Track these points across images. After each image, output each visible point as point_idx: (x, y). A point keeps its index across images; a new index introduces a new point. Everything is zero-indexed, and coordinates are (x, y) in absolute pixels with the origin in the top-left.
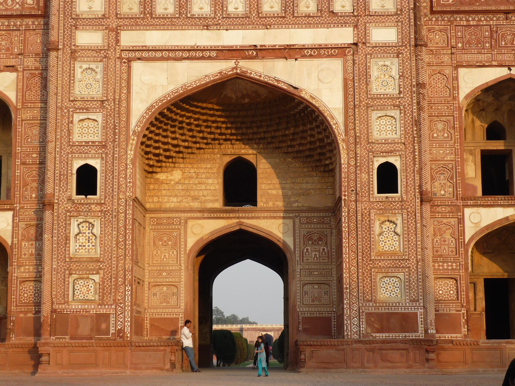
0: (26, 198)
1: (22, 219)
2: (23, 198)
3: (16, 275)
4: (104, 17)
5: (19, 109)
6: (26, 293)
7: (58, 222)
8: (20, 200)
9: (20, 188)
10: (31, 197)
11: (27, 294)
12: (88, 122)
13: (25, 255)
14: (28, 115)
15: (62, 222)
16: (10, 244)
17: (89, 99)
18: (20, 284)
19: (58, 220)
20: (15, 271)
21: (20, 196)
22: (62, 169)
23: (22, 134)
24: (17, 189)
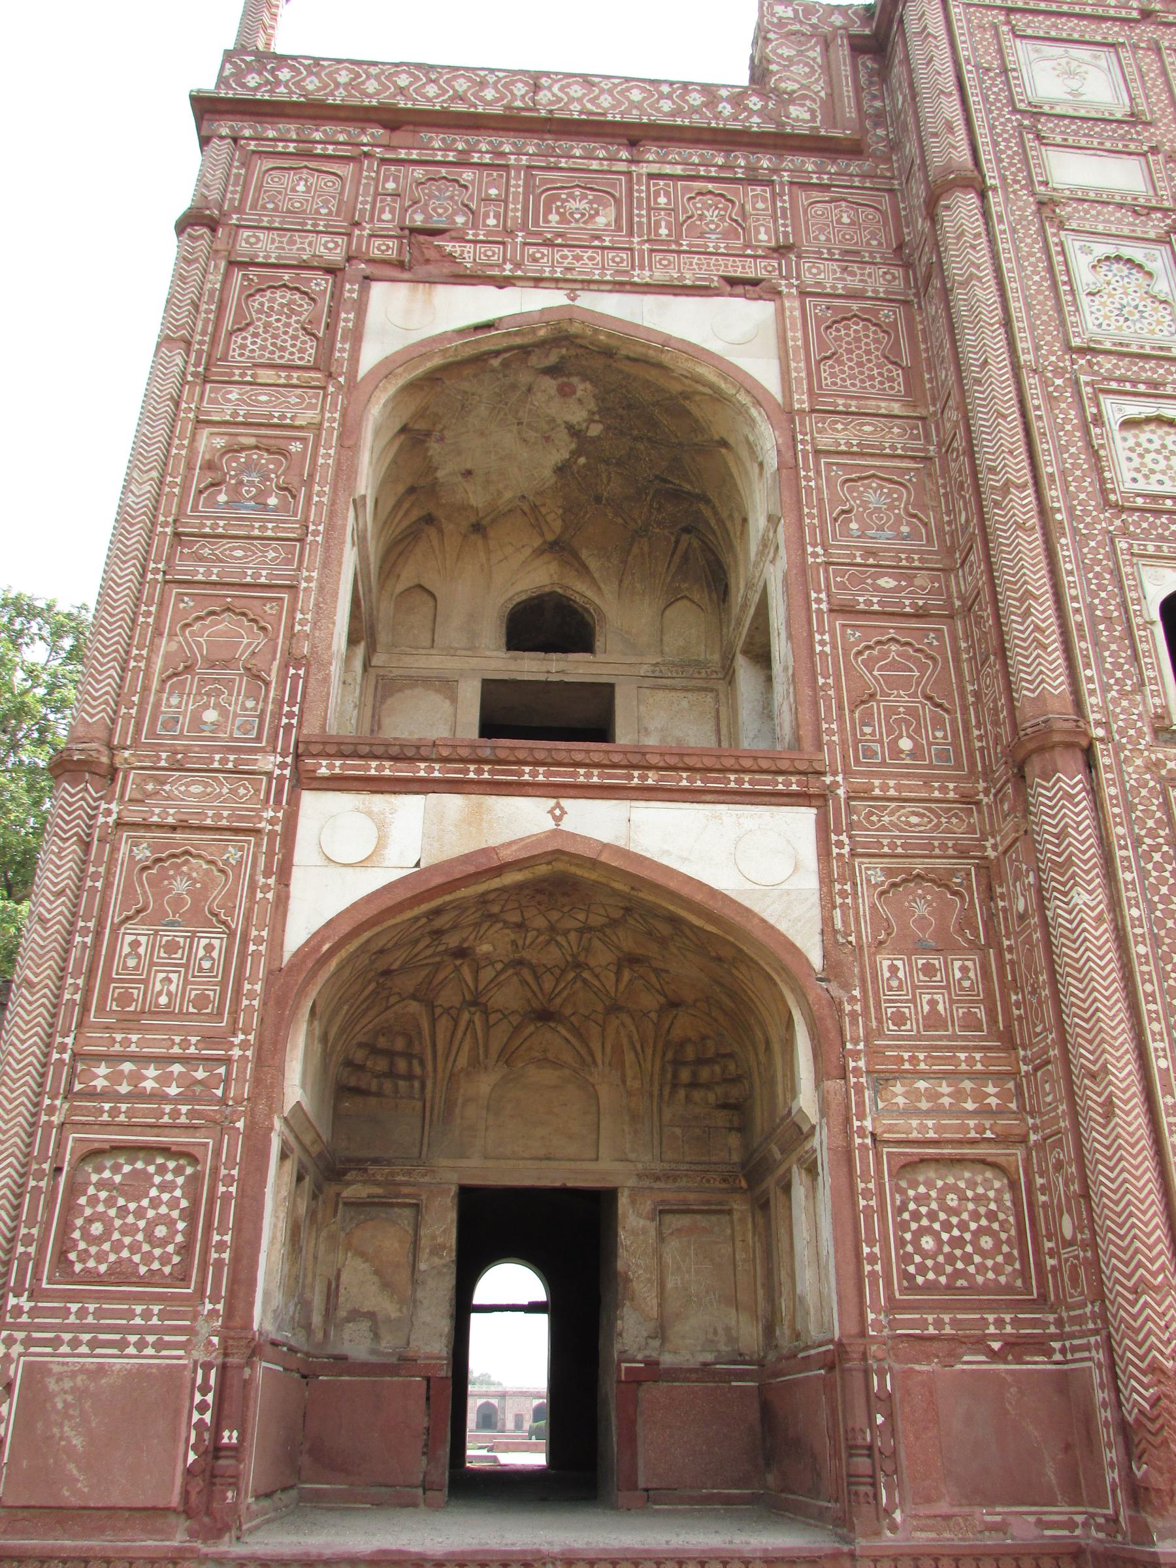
0: (869, 753)
1: (865, 845)
2: (856, 750)
3: (868, 1124)
4: (1134, 119)
5: (802, 411)
6: (928, 1230)
7: (1131, 831)
8: (845, 757)
9: (840, 708)
10: (896, 752)
11: (936, 1236)
12: (1160, 432)
13: (899, 1019)
14: (839, 436)
15: (1152, 833)
16: (816, 959)
17: (1148, 351)
18: (895, 1175)
19: (1130, 824)
20: (861, 1104)
21: (843, 742)
22: (1094, 594)
23: (821, 500)
24: (828, 708)
